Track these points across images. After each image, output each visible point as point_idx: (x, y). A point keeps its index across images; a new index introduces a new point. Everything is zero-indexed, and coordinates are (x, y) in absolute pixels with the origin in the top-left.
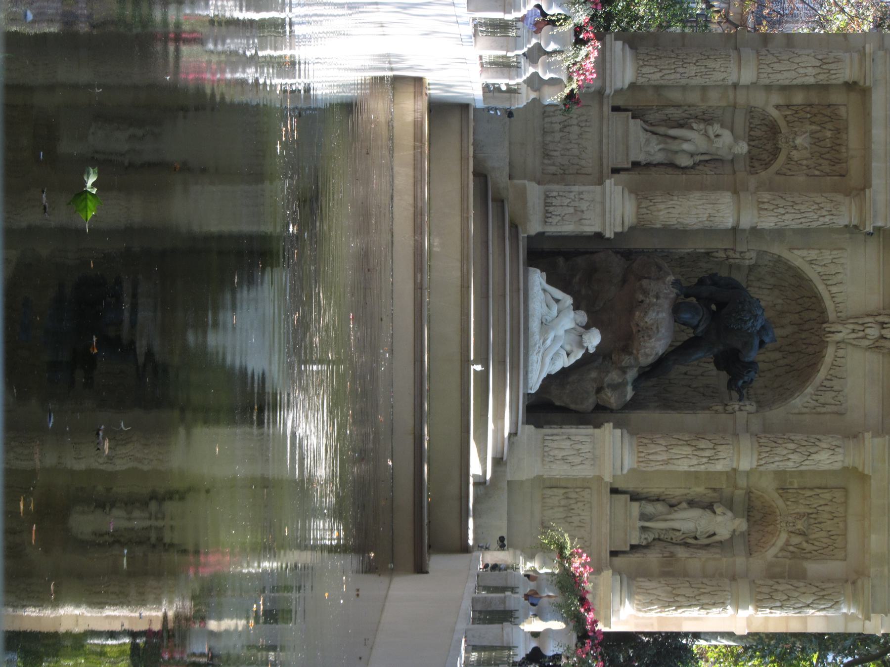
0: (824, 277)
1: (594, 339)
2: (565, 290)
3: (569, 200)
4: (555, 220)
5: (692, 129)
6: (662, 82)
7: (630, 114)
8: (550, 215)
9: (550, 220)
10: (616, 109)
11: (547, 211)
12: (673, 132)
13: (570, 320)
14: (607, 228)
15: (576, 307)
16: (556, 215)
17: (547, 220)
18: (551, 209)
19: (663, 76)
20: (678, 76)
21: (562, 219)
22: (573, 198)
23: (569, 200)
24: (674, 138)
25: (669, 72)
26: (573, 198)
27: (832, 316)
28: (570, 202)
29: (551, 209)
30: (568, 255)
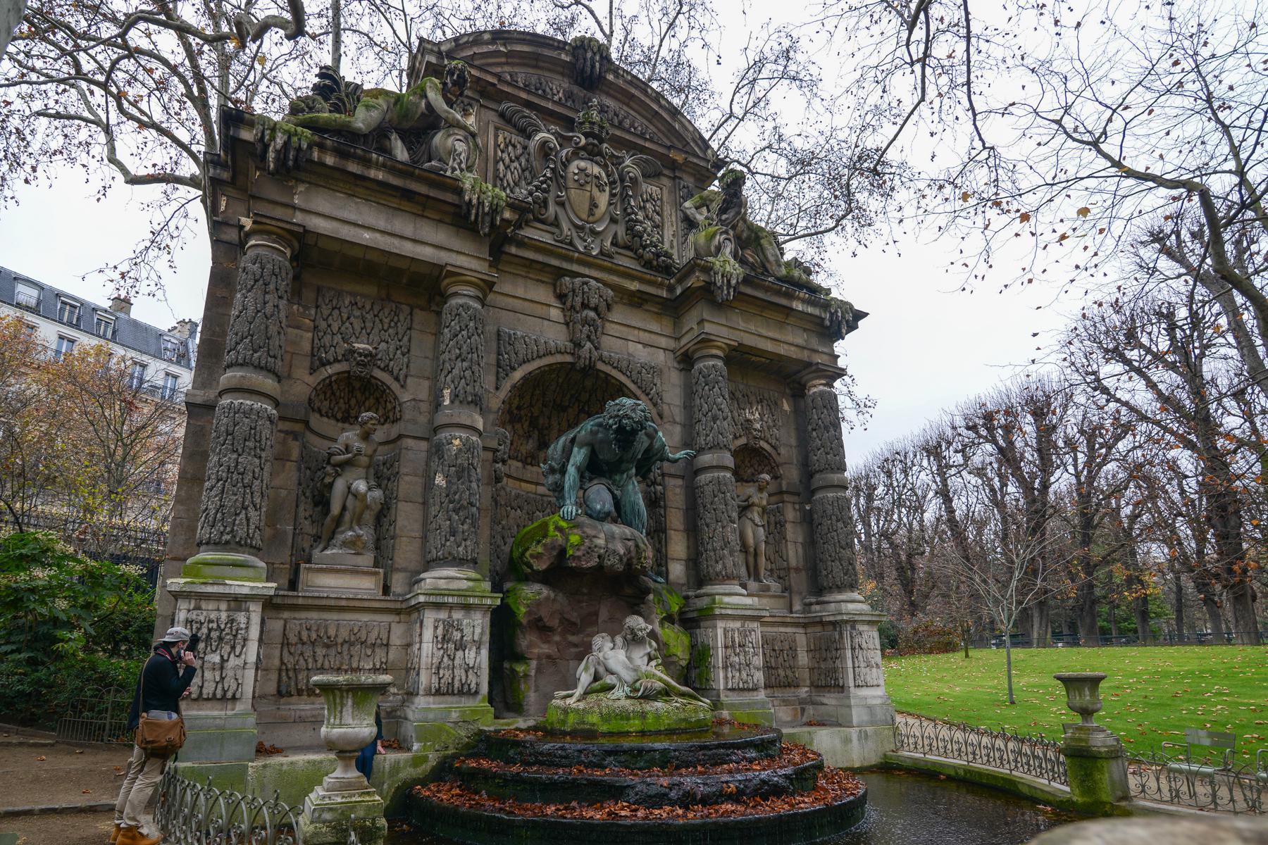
0: (529, 357)
3: (446, 659)
4: (472, 679)
5: (331, 485)
6: (264, 509)
7: (303, 565)
8: (466, 687)
9: (473, 686)
10: (293, 585)
11: (461, 693)
12: (335, 509)
14: (489, 602)
15: (586, 649)
16: (467, 676)
17: (473, 691)
18: (457, 684)
19: (255, 506)
20: (257, 483)
21: (473, 668)
22: (442, 652)
23: (446, 659)
24: (344, 508)
25: (249, 496)
26: (442, 652)
27: (568, 359)
28: (449, 656)
29: (457, 684)
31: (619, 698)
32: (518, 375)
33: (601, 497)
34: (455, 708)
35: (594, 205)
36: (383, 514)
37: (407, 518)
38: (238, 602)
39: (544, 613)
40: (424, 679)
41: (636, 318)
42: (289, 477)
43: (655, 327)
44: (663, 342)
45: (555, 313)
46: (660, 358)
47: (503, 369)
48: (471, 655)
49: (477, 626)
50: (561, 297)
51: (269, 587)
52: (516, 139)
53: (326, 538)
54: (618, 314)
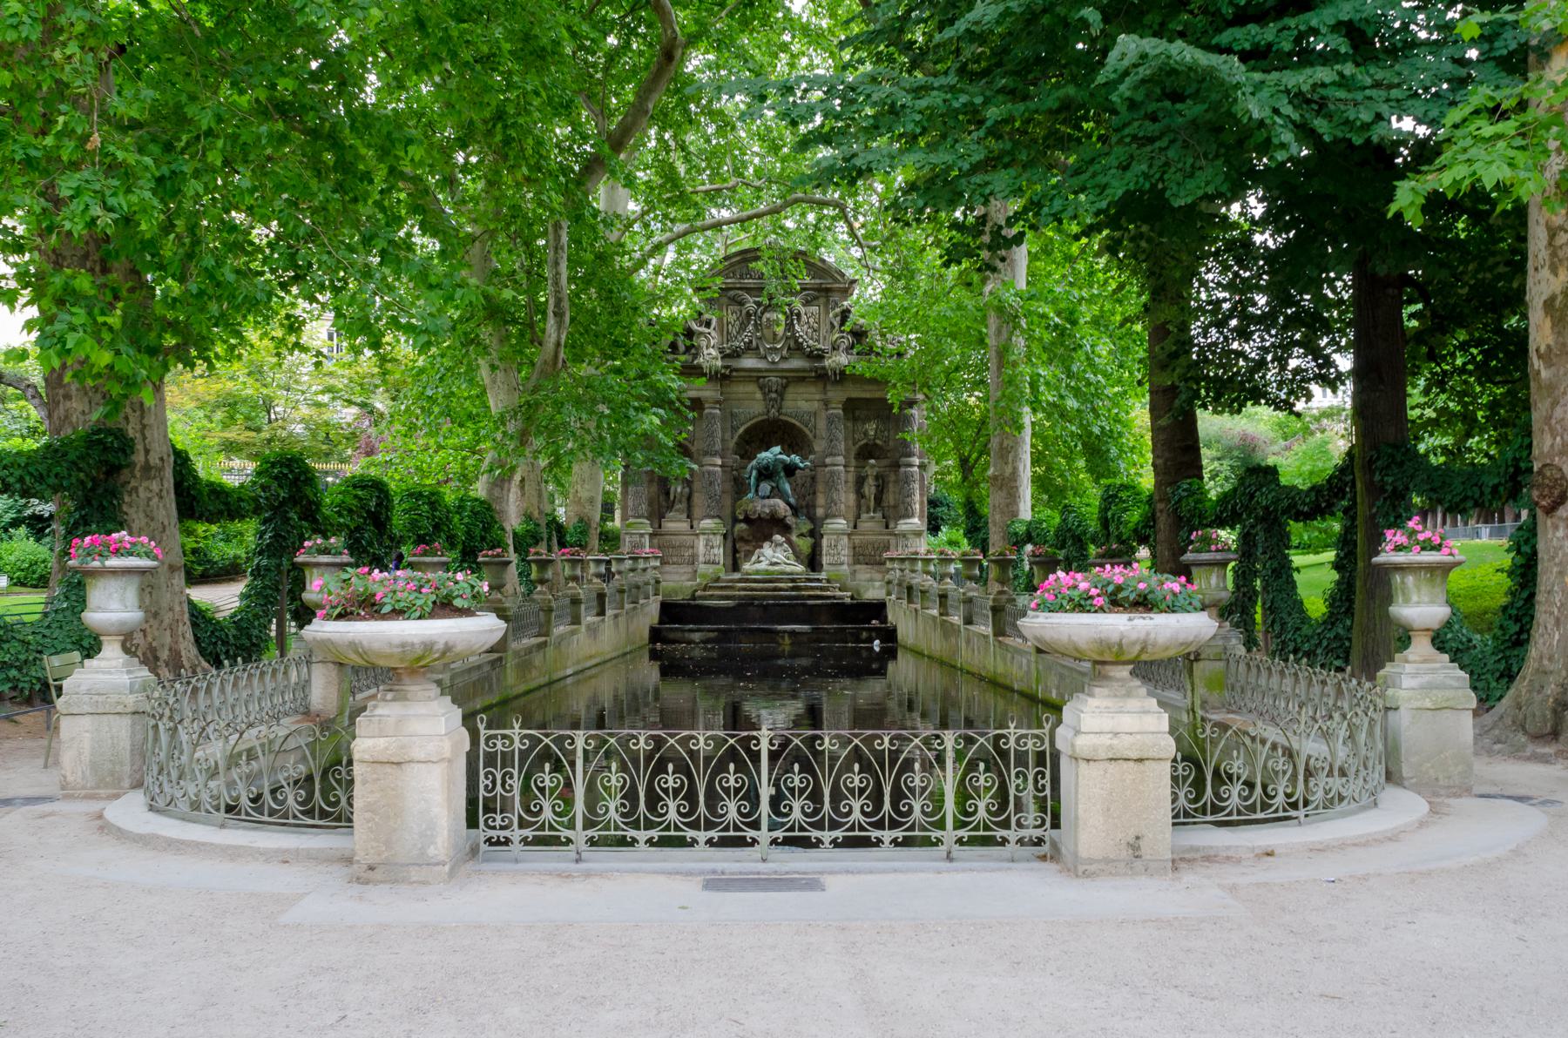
1: (778, 538)
2: (752, 553)
13: (767, 550)
30: (735, 551)
31: (763, 566)
32: (741, 430)
33: (766, 487)
34: (711, 569)
35: (775, 334)
36: (689, 498)
37: (698, 499)
38: (642, 535)
39: (745, 535)
40: (701, 559)
41: (801, 389)
42: (654, 488)
43: (812, 389)
44: (817, 397)
45: (759, 395)
46: (816, 404)
47: (734, 429)
48: (716, 551)
49: (718, 540)
50: (761, 388)
51: (650, 530)
52: (736, 308)
53: (670, 507)
54: (790, 389)
